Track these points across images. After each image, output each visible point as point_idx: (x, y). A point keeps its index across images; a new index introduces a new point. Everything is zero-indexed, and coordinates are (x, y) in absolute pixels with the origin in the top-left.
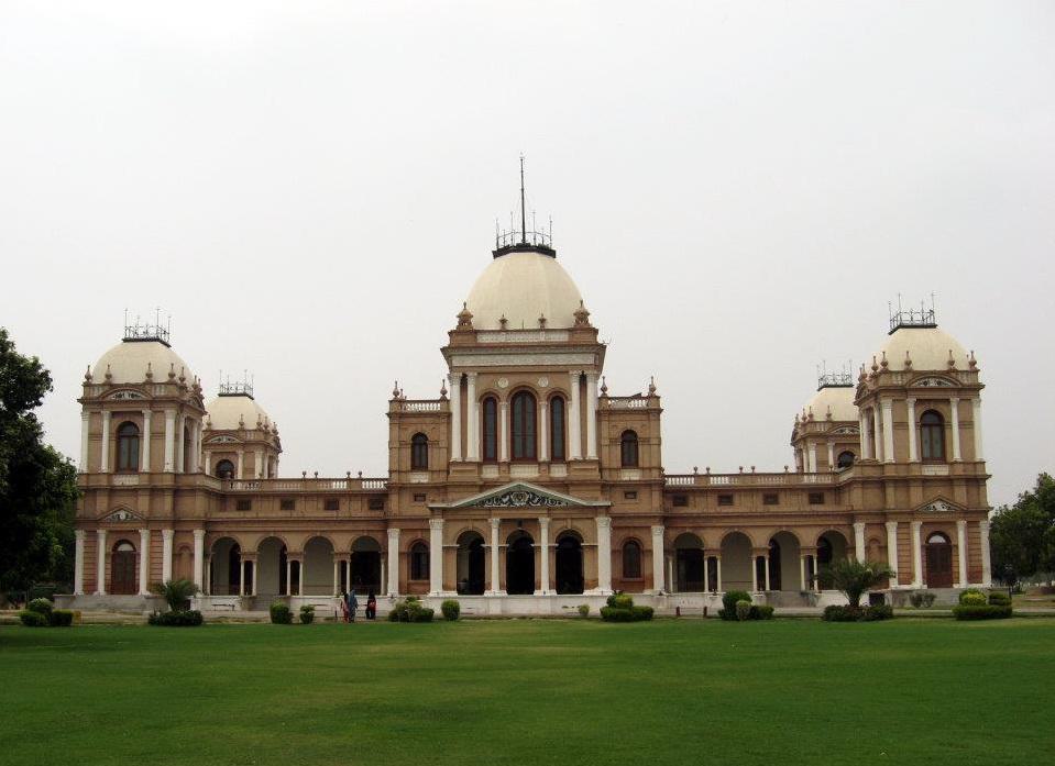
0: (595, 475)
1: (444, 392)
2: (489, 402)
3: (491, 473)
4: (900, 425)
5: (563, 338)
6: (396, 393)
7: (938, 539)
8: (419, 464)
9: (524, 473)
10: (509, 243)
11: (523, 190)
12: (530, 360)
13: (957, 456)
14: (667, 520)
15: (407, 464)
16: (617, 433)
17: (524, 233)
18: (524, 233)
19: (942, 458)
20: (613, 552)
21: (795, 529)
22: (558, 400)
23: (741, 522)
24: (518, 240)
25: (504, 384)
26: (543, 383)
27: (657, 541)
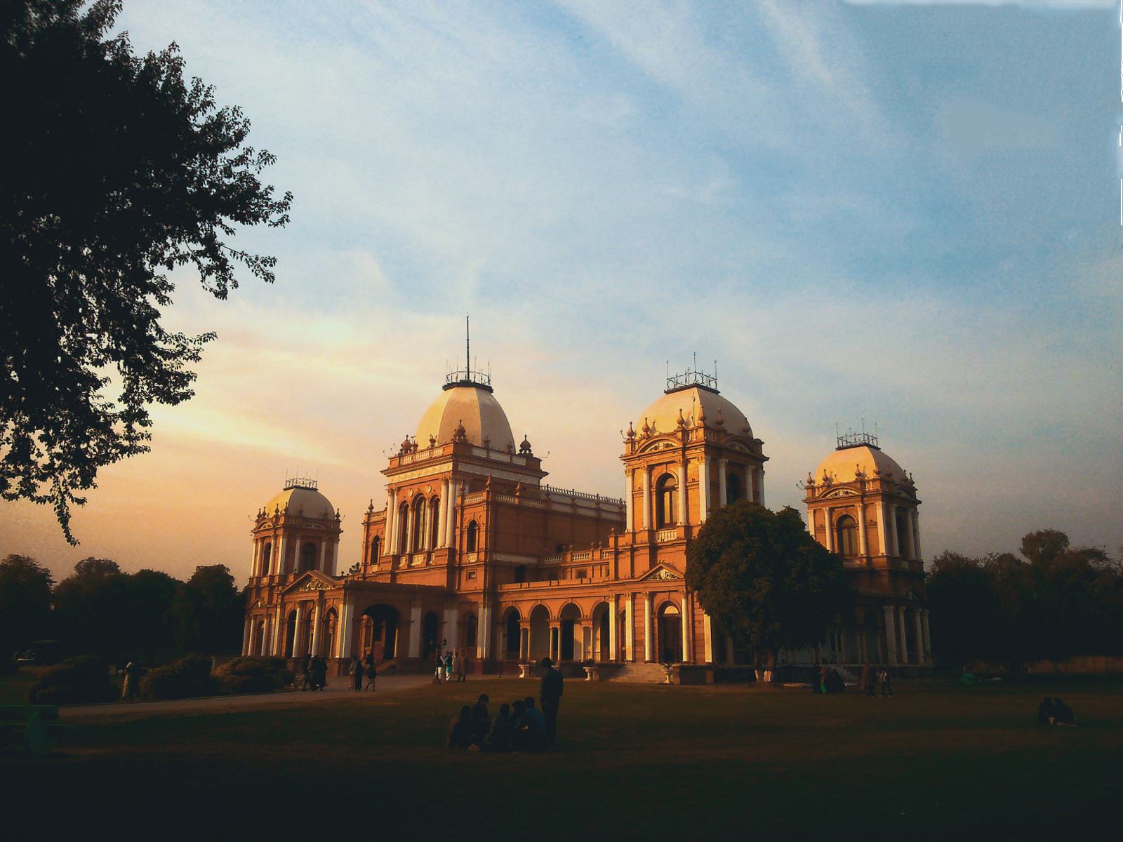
0: (444, 561)
1: (387, 504)
2: (403, 509)
3: (403, 562)
4: (636, 493)
5: (438, 452)
6: (371, 508)
7: (670, 610)
8: (374, 561)
9: (419, 560)
10: (454, 381)
11: (468, 340)
12: (423, 473)
13: (681, 519)
14: (492, 594)
15: (369, 561)
16: (466, 524)
17: (468, 372)
18: (468, 372)
19: (672, 525)
20: (459, 623)
21: (578, 600)
22: (435, 502)
23: (542, 595)
24: (462, 377)
25: (410, 493)
26: (427, 490)
27: (483, 614)
